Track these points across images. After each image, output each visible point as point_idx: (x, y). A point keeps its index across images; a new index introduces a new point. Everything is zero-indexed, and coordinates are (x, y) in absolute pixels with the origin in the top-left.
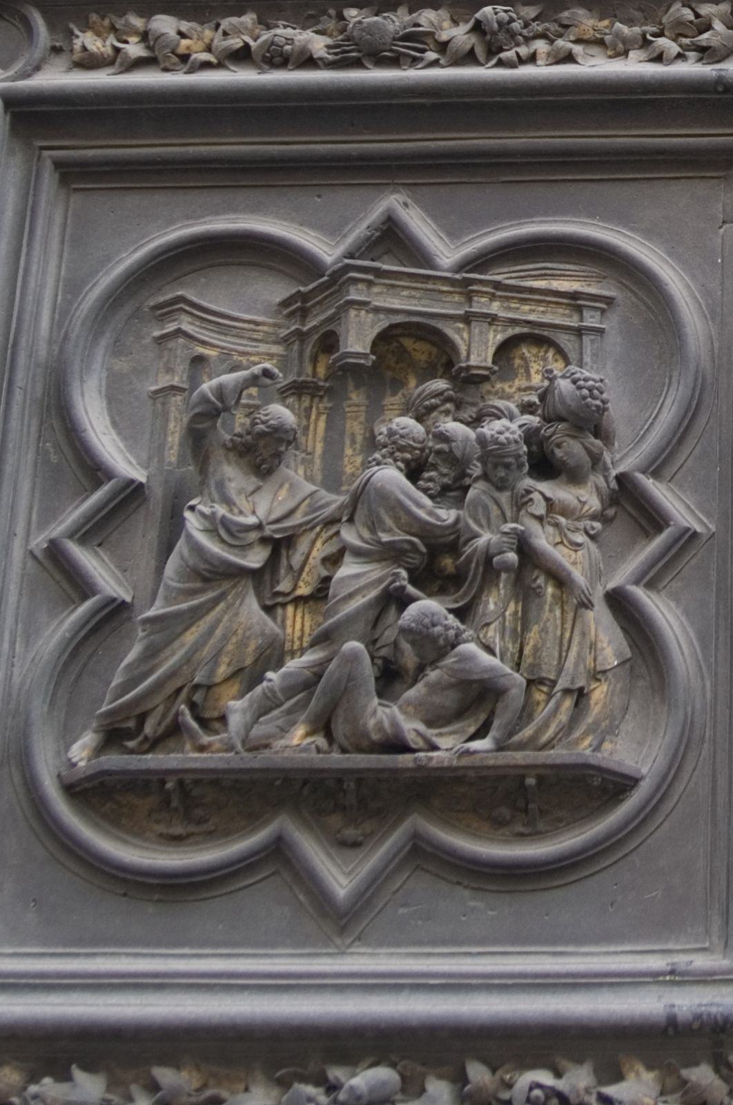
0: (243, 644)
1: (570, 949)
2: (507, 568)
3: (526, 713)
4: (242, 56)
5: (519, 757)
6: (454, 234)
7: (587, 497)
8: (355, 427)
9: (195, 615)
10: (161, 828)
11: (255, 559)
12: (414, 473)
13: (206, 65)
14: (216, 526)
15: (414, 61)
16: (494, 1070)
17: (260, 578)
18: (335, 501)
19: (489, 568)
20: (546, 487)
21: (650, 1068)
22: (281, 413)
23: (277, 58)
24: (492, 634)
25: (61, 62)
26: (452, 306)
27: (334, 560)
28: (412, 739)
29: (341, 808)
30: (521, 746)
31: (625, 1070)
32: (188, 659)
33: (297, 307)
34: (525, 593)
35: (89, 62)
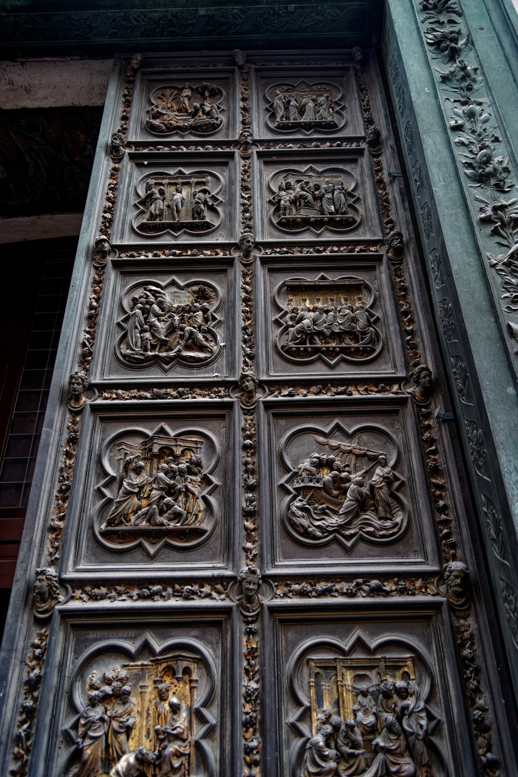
0: (134, 506)
2: (183, 492)
3: (187, 519)
4: (134, 397)
5: (185, 527)
6: (173, 430)
7: (198, 478)
8: (155, 466)
9: (125, 501)
11: (136, 490)
12: (166, 474)
13: (128, 399)
14: (129, 484)
15: (166, 398)
17: (138, 494)
18: (151, 479)
19: (180, 492)
20: (190, 477)
22: (141, 463)
23: (141, 398)
24: (180, 504)
25: (101, 398)
26: (173, 443)
27: (151, 490)
28: (165, 523)
30: (186, 525)
32: (124, 509)
33: (144, 444)
34: (186, 496)
35: (106, 398)
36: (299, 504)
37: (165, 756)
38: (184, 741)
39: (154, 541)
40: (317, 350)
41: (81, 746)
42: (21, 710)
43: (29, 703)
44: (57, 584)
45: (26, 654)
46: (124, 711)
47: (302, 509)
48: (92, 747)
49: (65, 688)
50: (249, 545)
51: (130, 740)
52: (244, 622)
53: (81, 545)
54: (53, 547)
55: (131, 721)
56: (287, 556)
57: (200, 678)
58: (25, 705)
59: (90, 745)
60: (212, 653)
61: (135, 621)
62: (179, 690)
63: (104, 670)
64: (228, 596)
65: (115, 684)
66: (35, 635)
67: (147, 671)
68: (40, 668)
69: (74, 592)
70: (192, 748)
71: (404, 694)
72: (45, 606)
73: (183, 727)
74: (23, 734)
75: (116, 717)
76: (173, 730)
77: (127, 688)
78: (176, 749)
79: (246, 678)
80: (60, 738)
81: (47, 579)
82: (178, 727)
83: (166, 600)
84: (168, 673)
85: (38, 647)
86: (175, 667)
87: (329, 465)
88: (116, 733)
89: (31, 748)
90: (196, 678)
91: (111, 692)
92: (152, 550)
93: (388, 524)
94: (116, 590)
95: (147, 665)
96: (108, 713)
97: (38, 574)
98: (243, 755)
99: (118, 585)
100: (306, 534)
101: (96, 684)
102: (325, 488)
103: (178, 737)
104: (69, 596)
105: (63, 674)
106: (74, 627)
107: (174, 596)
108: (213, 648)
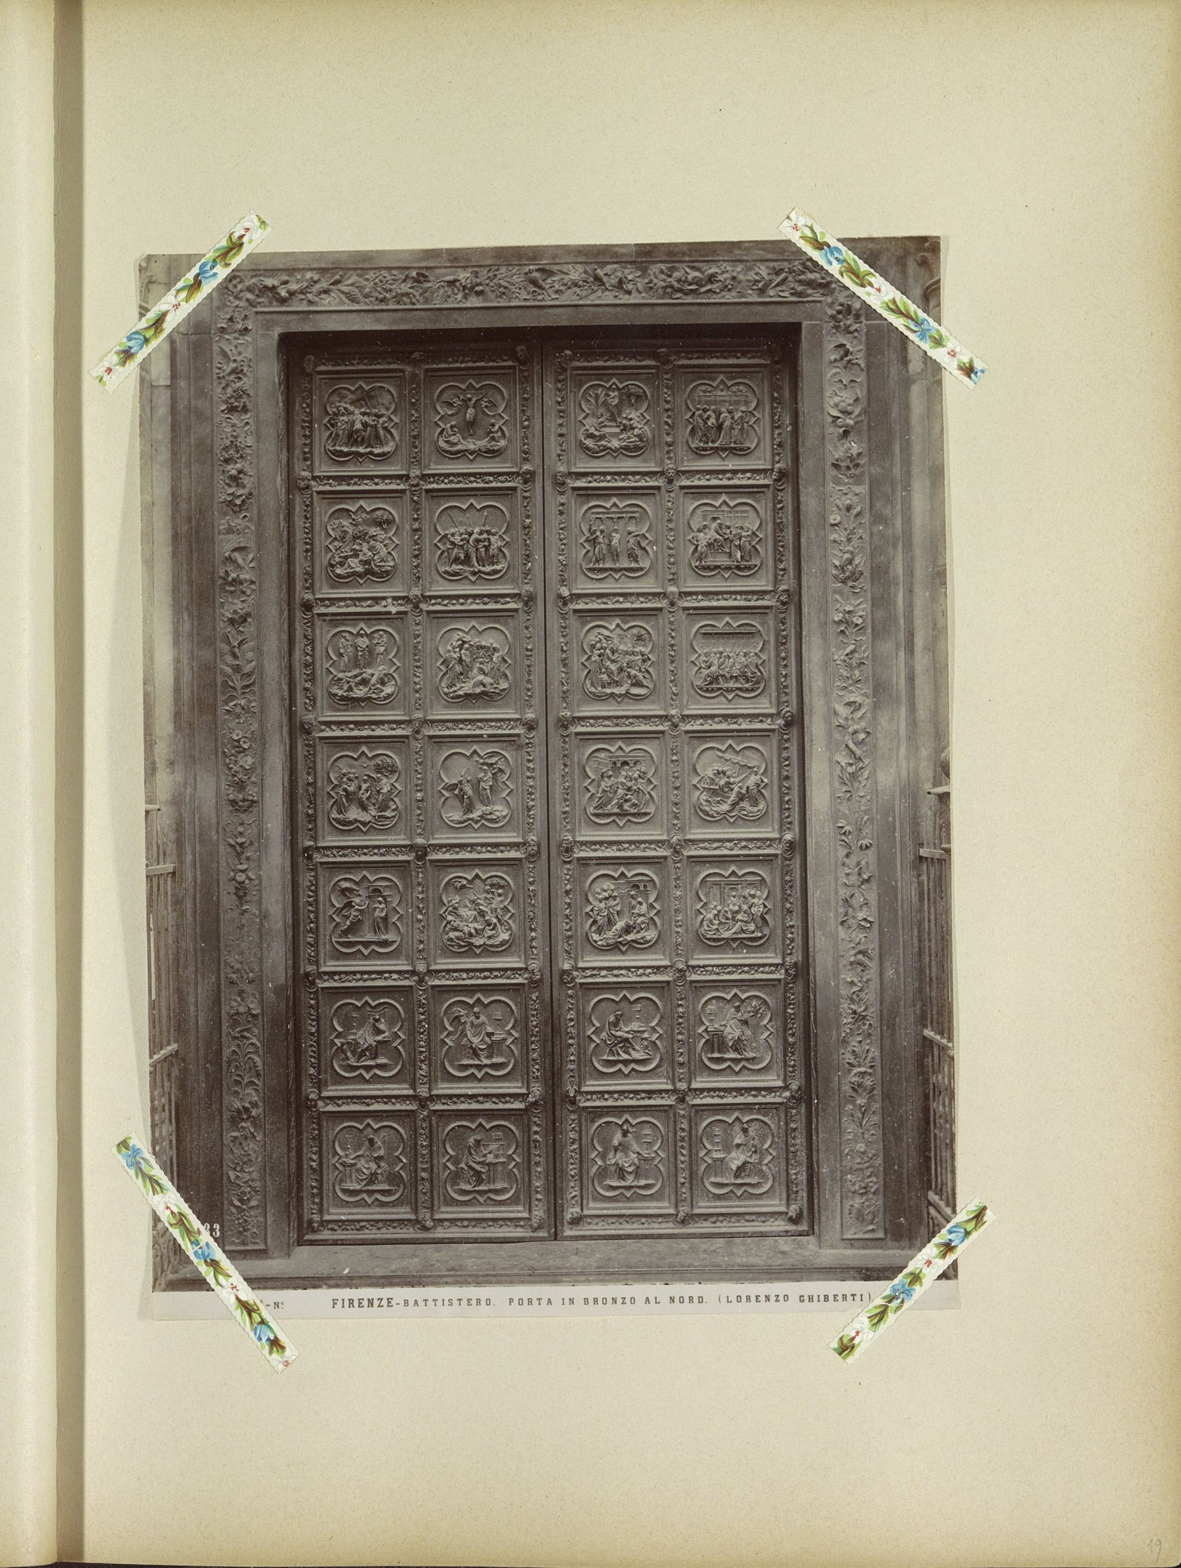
23: (604, 726)
36: (705, 798)
40: (721, 689)
47: (707, 801)
50: (676, 822)
56: (699, 827)
71: (753, 896)
87: (724, 773)
92: (621, 824)
93: (755, 809)
100: (707, 814)
102: (721, 788)
103: (643, 915)
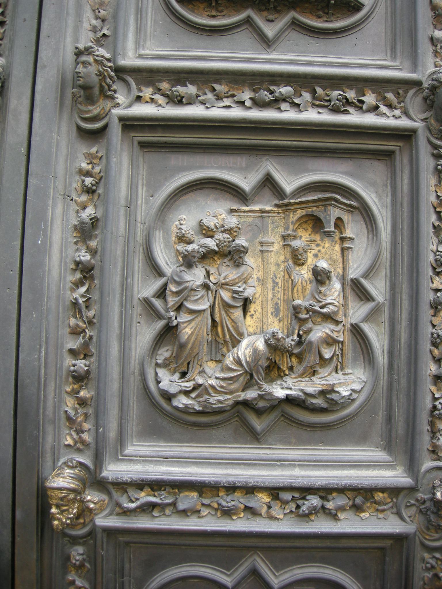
1: (343, 57)
10: (208, 13)
16: (324, 91)
21: (373, 93)
29: (267, 9)
31: (365, 93)
37: (310, 343)
38: (337, 323)
39: (271, 17)
41: (175, 323)
42: (73, 266)
43: (85, 257)
44: (113, 74)
45: (71, 185)
46: (239, 277)
48: (193, 324)
49: (138, 239)
51: (248, 318)
52: (433, 155)
53: (144, 15)
54: (97, 18)
55: (249, 293)
57: (357, 235)
58: (78, 259)
59: (190, 322)
60: (376, 201)
61: (248, 142)
62: (323, 251)
63: (200, 216)
64: (406, 113)
65: (219, 236)
66: (81, 157)
67: (270, 221)
68: (96, 207)
69: (140, 90)
70: (346, 333)
72: (95, 110)
73: (337, 304)
74: (81, 301)
75: (226, 284)
76: (322, 307)
77: (242, 241)
78: (327, 334)
79: (435, 240)
80: (138, 309)
81: (96, 61)
82: (330, 304)
83: (301, 111)
84: (305, 226)
85: (88, 174)
86: (322, 217)
88: (227, 306)
89: (95, 321)
90: (352, 236)
91: (216, 248)
92: (270, 31)
94: (214, 90)
95: (269, 212)
96: (212, 278)
97: (79, 53)
98: (429, 346)
99: (219, 82)
101: (189, 235)
103: (328, 318)
104: (132, 97)
105: (132, 217)
106: (143, 145)
107: (314, 105)
108: (377, 192)
